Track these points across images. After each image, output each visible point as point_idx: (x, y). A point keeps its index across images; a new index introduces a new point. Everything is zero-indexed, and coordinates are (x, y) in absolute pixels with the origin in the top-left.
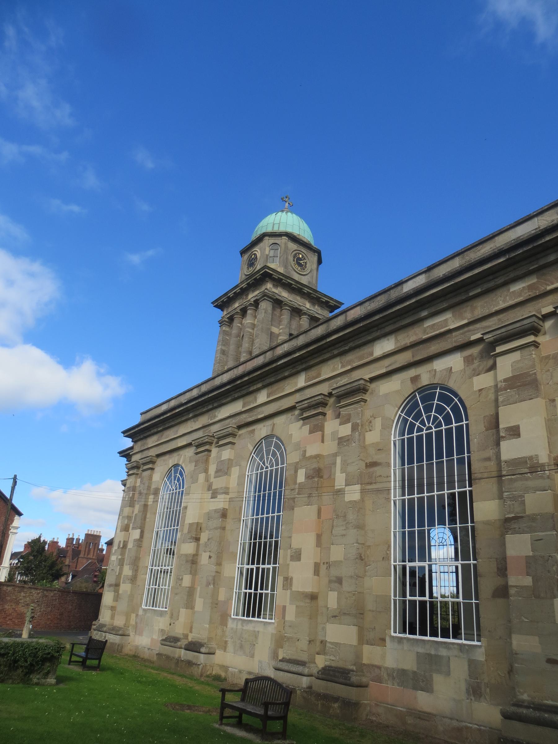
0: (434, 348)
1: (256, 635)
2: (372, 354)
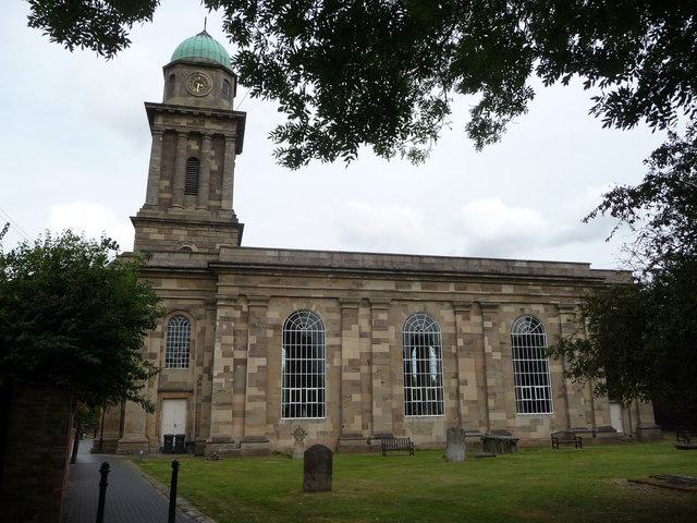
0: (533, 300)
1: (432, 423)
2: (501, 290)
